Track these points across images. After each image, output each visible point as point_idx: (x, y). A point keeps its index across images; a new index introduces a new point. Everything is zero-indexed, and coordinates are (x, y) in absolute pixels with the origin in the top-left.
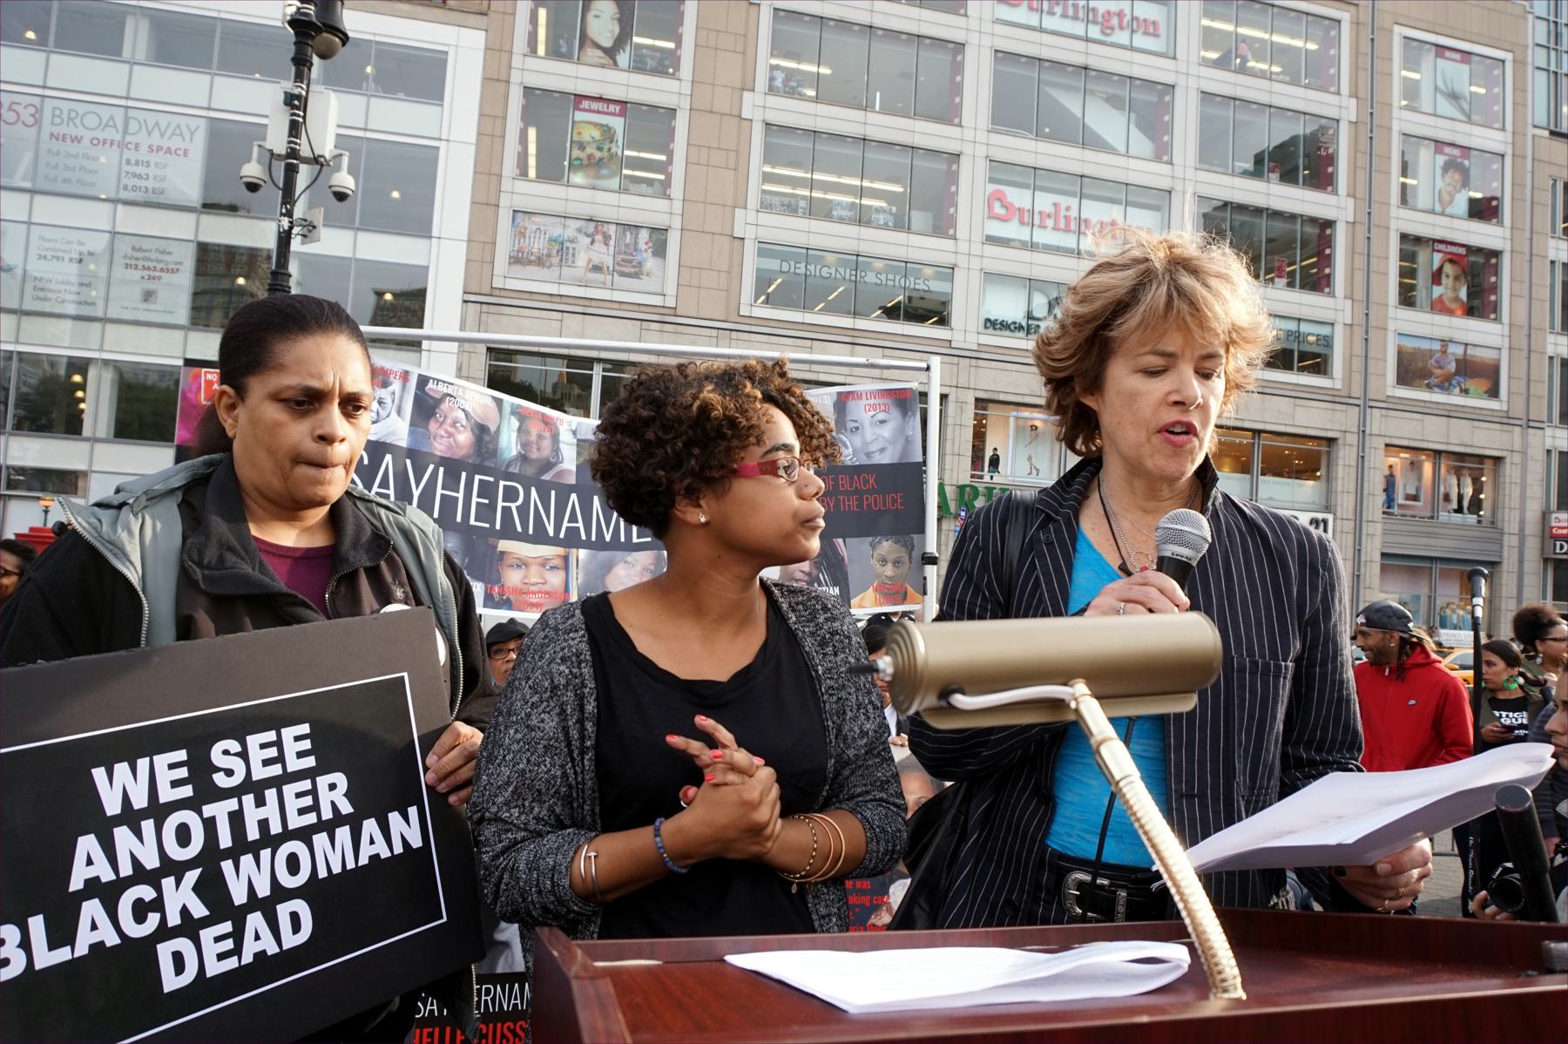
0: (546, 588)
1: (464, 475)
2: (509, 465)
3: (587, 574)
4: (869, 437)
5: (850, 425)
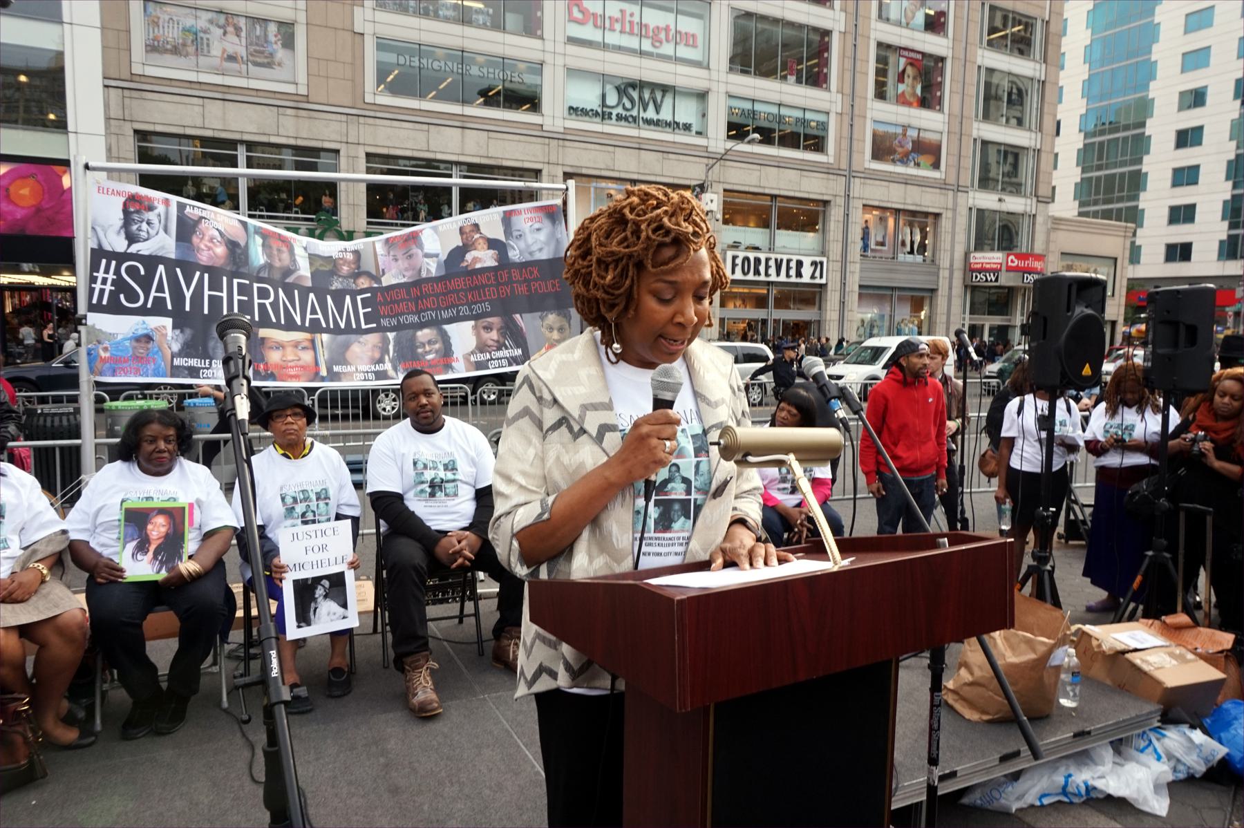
0: (301, 363)
1: (225, 279)
2: (259, 272)
3: (331, 351)
4: (530, 241)
5: (515, 234)
